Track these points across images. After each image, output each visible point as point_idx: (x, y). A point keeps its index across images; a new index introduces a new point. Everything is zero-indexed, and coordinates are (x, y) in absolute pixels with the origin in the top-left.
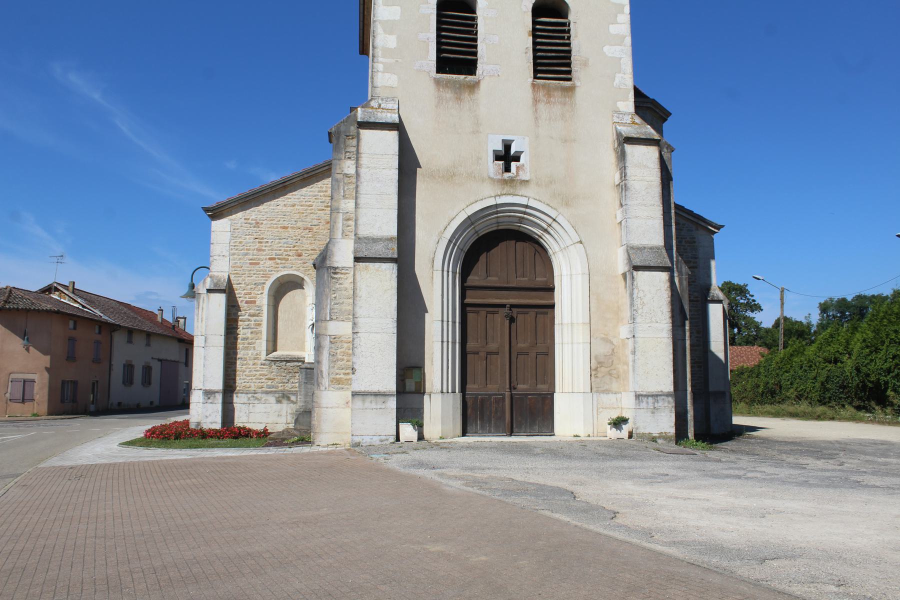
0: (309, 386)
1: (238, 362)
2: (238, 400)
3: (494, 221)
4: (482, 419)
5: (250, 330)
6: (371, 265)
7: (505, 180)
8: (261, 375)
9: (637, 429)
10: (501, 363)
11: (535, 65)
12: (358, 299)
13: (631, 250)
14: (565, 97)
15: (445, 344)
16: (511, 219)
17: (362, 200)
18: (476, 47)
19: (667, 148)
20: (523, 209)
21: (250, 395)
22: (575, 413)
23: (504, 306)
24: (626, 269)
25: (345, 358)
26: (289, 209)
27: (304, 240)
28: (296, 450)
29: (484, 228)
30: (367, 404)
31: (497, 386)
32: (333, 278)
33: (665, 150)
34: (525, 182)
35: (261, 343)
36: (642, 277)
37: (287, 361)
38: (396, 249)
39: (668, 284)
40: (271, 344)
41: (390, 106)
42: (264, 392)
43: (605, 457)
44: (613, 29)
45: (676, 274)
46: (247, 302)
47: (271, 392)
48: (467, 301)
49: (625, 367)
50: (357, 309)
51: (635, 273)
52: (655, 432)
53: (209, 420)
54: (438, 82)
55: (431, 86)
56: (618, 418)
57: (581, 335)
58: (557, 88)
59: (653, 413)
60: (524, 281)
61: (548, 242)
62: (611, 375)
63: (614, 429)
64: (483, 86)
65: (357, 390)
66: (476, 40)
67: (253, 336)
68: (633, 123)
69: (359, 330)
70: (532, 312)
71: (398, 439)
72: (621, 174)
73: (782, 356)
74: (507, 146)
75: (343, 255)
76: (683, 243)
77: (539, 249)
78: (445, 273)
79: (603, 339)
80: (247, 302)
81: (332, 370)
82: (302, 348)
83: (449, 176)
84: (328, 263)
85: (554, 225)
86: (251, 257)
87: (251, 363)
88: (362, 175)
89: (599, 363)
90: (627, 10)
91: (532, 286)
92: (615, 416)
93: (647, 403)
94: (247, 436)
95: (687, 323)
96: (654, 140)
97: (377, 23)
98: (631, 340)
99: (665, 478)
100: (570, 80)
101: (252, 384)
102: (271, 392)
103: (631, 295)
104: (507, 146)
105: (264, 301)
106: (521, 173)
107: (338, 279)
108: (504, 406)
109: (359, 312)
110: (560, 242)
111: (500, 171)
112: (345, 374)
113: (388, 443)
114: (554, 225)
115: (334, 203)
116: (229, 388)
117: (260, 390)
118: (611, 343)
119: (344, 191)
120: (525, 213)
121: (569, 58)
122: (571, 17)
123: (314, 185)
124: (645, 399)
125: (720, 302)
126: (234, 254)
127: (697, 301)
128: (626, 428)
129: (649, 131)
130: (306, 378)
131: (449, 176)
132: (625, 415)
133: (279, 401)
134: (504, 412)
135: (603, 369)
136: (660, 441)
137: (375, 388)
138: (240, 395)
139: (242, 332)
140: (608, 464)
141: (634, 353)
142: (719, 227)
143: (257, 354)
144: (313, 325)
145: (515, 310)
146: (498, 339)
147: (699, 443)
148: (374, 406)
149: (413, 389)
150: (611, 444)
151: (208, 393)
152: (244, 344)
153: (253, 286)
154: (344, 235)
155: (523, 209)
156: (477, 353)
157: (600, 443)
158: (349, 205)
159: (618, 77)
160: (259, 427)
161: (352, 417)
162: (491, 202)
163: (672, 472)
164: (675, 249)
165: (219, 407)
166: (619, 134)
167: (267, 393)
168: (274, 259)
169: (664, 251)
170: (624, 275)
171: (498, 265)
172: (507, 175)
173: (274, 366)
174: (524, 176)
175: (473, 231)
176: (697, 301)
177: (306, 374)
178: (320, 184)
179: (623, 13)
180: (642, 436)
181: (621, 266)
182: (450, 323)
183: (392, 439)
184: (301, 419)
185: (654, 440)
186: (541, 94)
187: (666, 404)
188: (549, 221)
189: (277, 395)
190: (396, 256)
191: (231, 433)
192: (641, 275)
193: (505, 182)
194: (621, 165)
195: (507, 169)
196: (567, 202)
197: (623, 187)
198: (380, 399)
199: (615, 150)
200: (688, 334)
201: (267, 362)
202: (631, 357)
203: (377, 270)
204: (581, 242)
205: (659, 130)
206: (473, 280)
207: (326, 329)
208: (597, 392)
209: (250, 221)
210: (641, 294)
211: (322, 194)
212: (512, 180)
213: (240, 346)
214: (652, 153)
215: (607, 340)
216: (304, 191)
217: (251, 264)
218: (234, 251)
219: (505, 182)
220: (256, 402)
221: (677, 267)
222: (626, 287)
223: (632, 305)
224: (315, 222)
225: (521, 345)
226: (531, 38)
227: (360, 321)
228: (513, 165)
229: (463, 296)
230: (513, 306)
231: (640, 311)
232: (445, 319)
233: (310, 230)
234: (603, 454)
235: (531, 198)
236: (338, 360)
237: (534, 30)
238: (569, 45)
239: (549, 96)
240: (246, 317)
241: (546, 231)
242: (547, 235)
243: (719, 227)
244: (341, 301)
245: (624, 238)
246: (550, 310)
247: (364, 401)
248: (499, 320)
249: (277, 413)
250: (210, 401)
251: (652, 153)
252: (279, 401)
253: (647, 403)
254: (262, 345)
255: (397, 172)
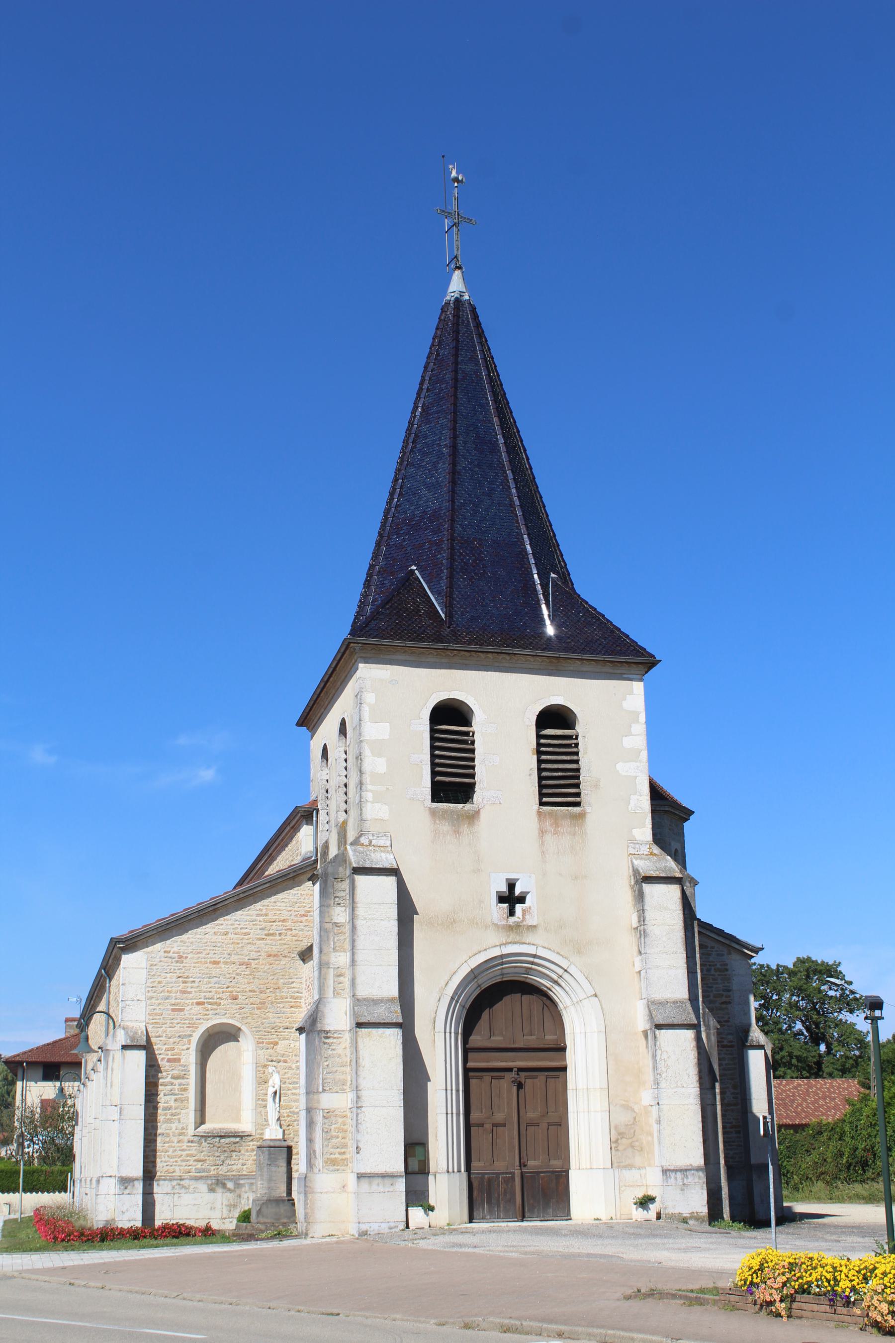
0: (273, 1169)
1: (159, 1139)
2: (160, 1189)
3: (499, 972)
4: (489, 1202)
5: (173, 1097)
6: (374, 1031)
7: (510, 926)
8: (188, 1155)
9: (665, 1208)
10: (508, 1136)
11: (541, 787)
12: (361, 1069)
13: (653, 1005)
14: (575, 826)
15: (449, 1116)
16: (516, 970)
17: (359, 957)
18: (473, 767)
19: (690, 882)
20: (531, 959)
21: (174, 1183)
22: (592, 1191)
23: (510, 1070)
24: (648, 1026)
25: (340, 1135)
26: (220, 938)
27: (240, 978)
28: (275, 1244)
29: (486, 981)
30: (374, 1187)
31: (505, 1163)
32: (325, 1043)
33: (688, 884)
34: (532, 928)
35: (188, 1114)
36: (665, 1035)
37: (221, 1137)
38: (399, 1011)
39: (694, 1043)
40: (199, 1113)
41: (382, 842)
42: (192, 1178)
43: (637, 1236)
44: (628, 742)
45: (703, 1029)
46: (169, 1061)
47: (201, 1178)
48: (470, 1064)
49: (650, 1138)
50: (360, 1080)
51: (657, 1032)
52: (686, 1213)
53: (126, 1216)
54: (433, 813)
55: (426, 817)
56: (644, 1196)
57: (598, 1102)
58: (564, 816)
59: (682, 1190)
60: (531, 1040)
61: (558, 994)
62: (633, 1147)
63: (640, 1210)
64: (483, 815)
65: (362, 1171)
66: (473, 760)
67: (178, 1104)
68: (652, 854)
69: (363, 1104)
70: (542, 1076)
71: (407, 1227)
72: (639, 917)
73: (874, 1105)
74: (511, 886)
75: (338, 1016)
76: (713, 972)
77: (548, 1002)
78: (448, 1035)
79: (622, 1106)
80: (169, 1061)
81: (326, 1150)
82: (238, 1119)
83: (450, 923)
84: (319, 1026)
85: (566, 976)
86: (173, 1001)
87: (175, 1139)
88: (359, 927)
89: (620, 1134)
90: (642, 718)
91: (542, 1046)
92: (640, 1195)
93: (676, 1178)
94: (188, 1235)
95: (717, 1085)
96: (675, 878)
97: (364, 743)
98: (655, 1108)
99: (698, 1249)
100: (578, 804)
101: (177, 1168)
102: (201, 1178)
103: (654, 1056)
104: (511, 886)
105: (191, 1058)
106: (527, 917)
107: (330, 1044)
108: (513, 1187)
109: (363, 1084)
110: (572, 996)
111: (505, 916)
112: (340, 1154)
113: (398, 1230)
114: (566, 976)
115: (324, 957)
116: (149, 1175)
117: (187, 1176)
118: (633, 1110)
119: (334, 943)
120: (532, 963)
121: (578, 777)
122: (579, 728)
123: (252, 907)
124: (673, 1175)
125: (761, 1047)
126: (152, 998)
127: (732, 1046)
128: (654, 1208)
129: (670, 865)
130: (269, 1159)
131: (450, 923)
132: (651, 1193)
133: (211, 1190)
134: (514, 1194)
135: (624, 1141)
136: (691, 1222)
137: (382, 1169)
138: (161, 1182)
139: (163, 1100)
140: (641, 1241)
141: (659, 1122)
142: (757, 950)
143: (183, 1128)
144: (275, 1093)
145: (523, 1074)
146: (505, 1110)
147: (735, 1224)
148: (381, 1189)
149: (416, 1169)
150: (639, 1225)
151: (125, 1182)
152: (165, 1115)
153: (177, 1040)
154: (336, 993)
155: (531, 959)
156: (482, 1125)
157: (627, 1225)
158: (341, 959)
159: (634, 798)
160: (202, 1224)
161: (348, 1201)
162: (496, 952)
163: (704, 1246)
164: (701, 999)
165: (138, 1199)
166: (636, 872)
167: (196, 1179)
168: (203, 1003)
169: (689, 1005)
170: (645, 1033)
171: (505, 1022)
172: (512, 920)
173: (204, 1144)
174: (530, 921)
175: (476, 985)
176: (732, 1046)
177: (270, 1154)
178: (258, 905)
179: (638, 722)
180: (672, 1217)
181: (642, 1023)
182: (454, 1092)
183: (402, 1226)
184: (264, 1210)
185: (685, 1221)
186: (548, 823)
187: (697, 1180)
188: (560, 971)
189: (209, 1182)
190: (401, 1021)
191: (149, 1232)
192: (663, 1034)
193: (510, 928)
194: (639, 907)
195: (512, 913)
196: (579, 949)
197: (641, 931)
198: (388, 1181)
199: (632, 887)
200: (718, 1098)
201: (196, 1139)
202: (655, 1127)
203: (381, 1037)
204: (596, 995)
205: (680, 857)
206: (476, 1039)
207: (318, 1102)
208: (619, 1167)
209: (171, 954)
210: (665, 1056)
211: (261, 918)
212: (517, 927)
213: (161, 1118)
214: (674, 891)
215: (627, 1108)
216: (238, 915)
217: (173, 1010)
218: (150, 994)
219: (510, 928)
220: (183, 1191)
221: (704, 1021)
222: (647, 1047)
223: (655, 1068)
224: (254, 955)
225: (531, 1115)
226: (535, 757)
227: (364, 1094)
228: (519, 907)
229: (465, 1060)
230: (520, 1070)
231: (664, 1076)
232: (449, 1088)
233: (248, 965)
234: (633, 1234)
235: (539, 944)
236: (332, 1137)
237: (539, 745)
238: (577, 762)
239: (556, 824)
240: (168, 1079)
241: (556, 982)
242: (557, 988)
243: (757, 950)
244: (334, 1069)
245: (644, 990)
246: (561, 1073)
247: (370, 1183)
248: (505, 1085)
249: (209, 1206)
250: (127, 1191)
251: (674, 891)
252: (211, 1190)
253: (676, 1178)
254: (189, 1115)
255: (396, 923)
